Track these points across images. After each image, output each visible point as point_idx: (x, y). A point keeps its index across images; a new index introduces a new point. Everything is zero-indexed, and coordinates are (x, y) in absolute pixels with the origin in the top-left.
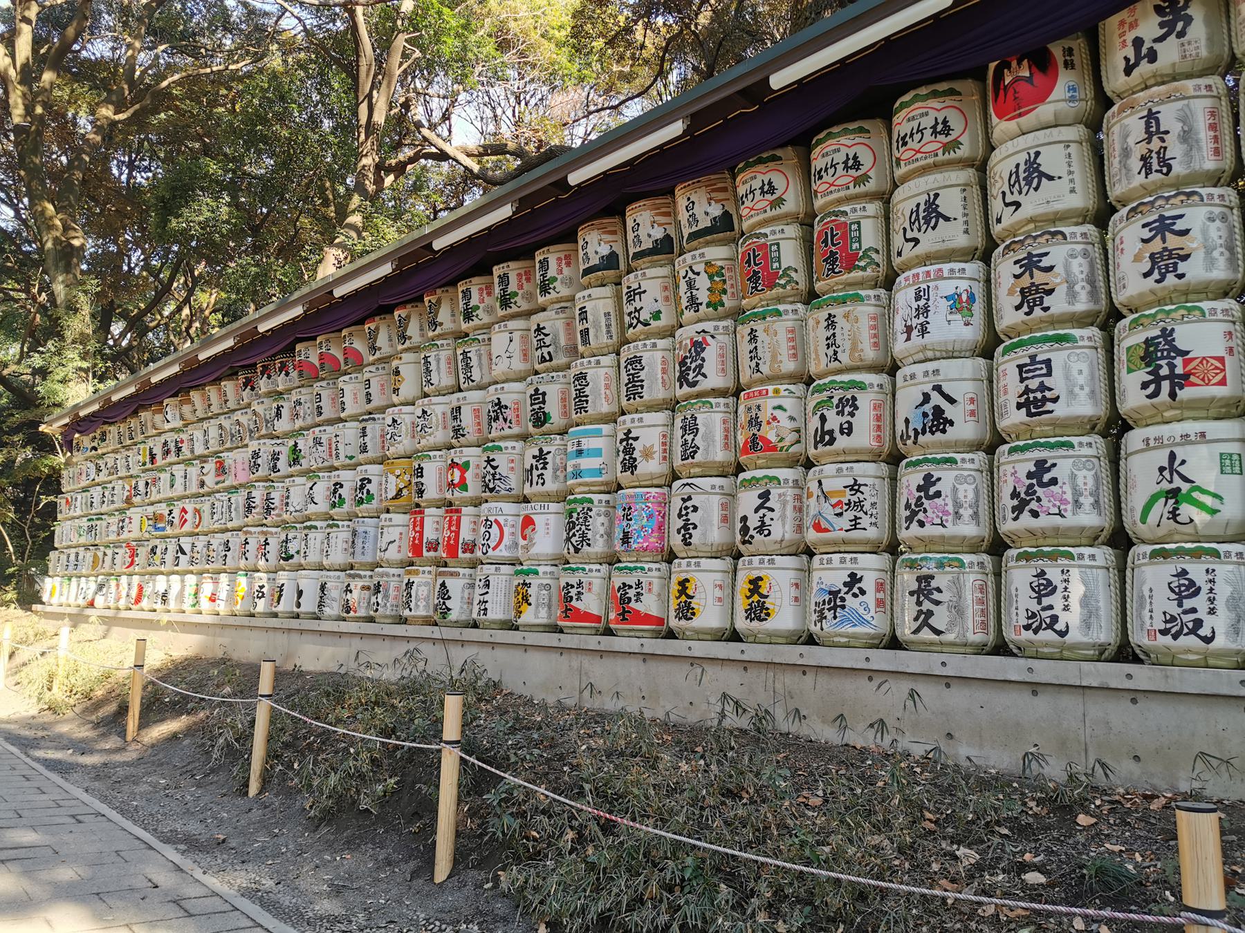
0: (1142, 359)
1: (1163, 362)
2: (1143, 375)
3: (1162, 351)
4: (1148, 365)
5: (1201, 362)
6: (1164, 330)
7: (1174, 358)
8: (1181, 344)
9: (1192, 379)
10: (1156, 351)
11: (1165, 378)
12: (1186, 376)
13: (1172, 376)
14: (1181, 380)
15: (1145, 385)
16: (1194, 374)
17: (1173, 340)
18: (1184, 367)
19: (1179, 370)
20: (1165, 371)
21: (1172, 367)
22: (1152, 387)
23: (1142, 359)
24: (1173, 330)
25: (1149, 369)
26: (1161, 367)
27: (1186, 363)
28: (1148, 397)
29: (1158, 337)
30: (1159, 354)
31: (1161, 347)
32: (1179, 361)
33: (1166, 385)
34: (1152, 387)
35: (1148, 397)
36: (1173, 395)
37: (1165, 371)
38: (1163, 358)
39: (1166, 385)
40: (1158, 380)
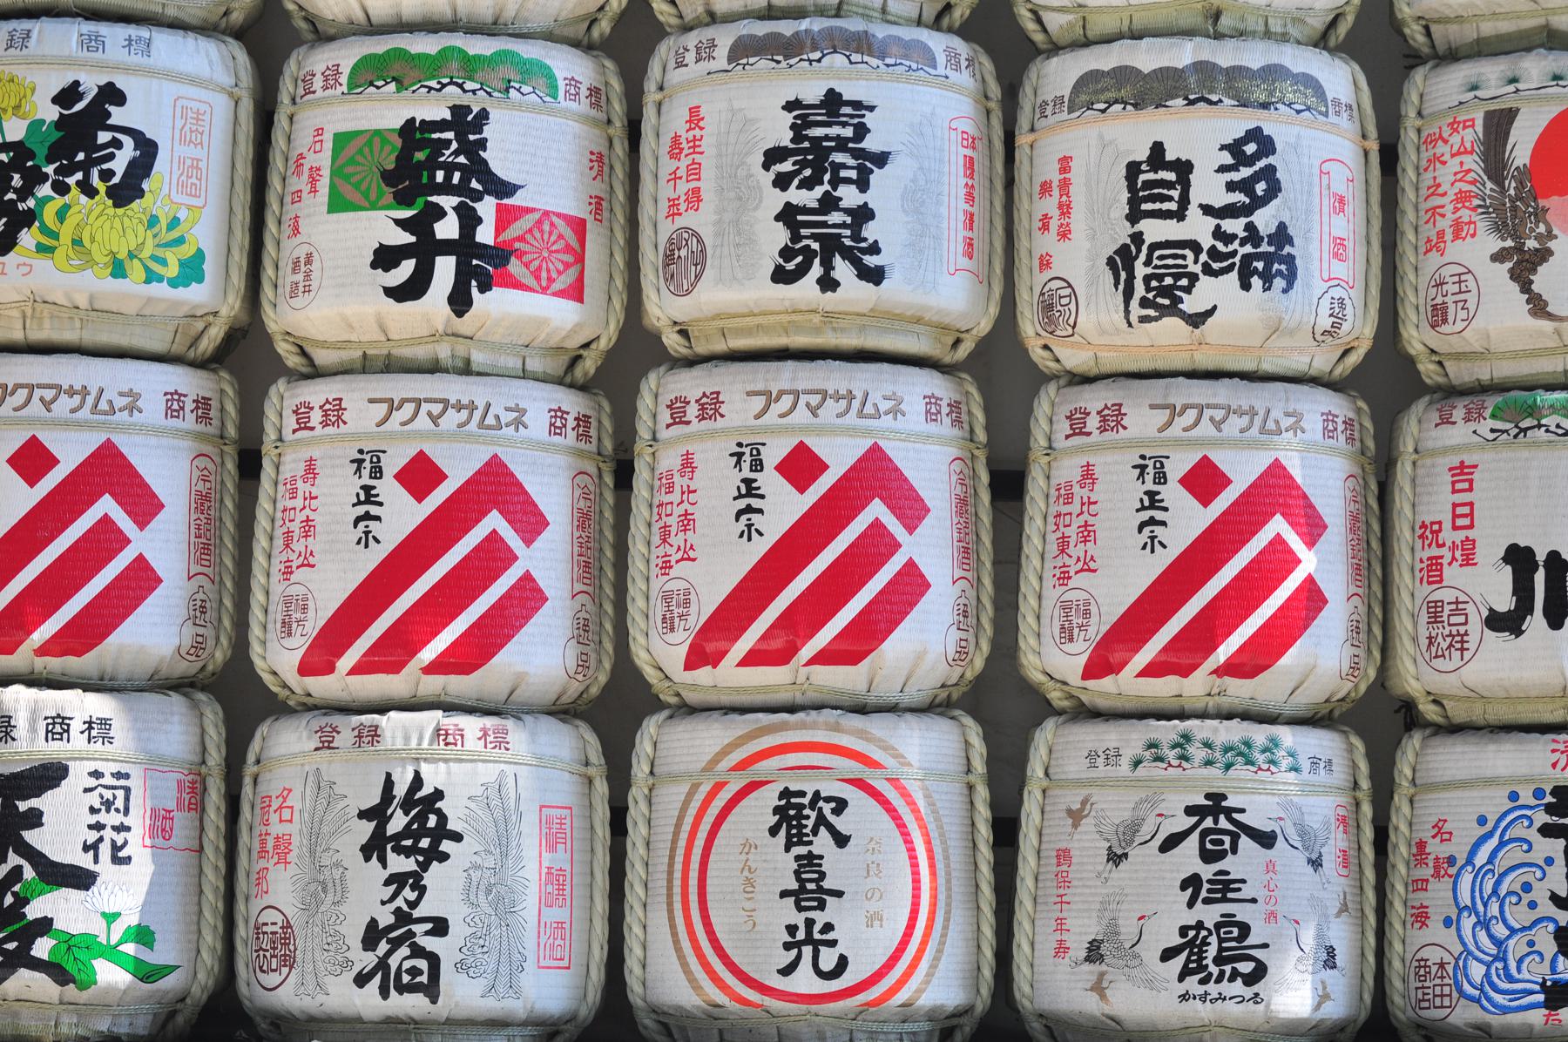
0: (388, 177)
1: (448, 202)
2: (383, 226)
3: (450, 168)
4: (403, 200)
5: (539, 223)
6: (459, 111)
7: (478, 197)
8: (498, 160)
9: (514, 267)
10: (432, 164)
11: (446, 247)
12: (500, 254)
13: (465, 247)
14: (480, 268)
15: (385, 258)
16: (520, 255)
17: (482, 144)
18: (499, 229)
19: (485, 234)
20: (447, 229)
21: (469, 220)
22: (407, 267)
23: (388, 177)
24: (483, 115)
25: (407, 213)
26: (440, 213)
27: (506, 217)
28: (390, 292)
29: (441, 125)
30: (440, 176)
31: (447, 156)
32: (487, 208)
33: (445, 267)
34: (407, 267)
35: (390, 292)
36: (460, 301)
37: (447, 229)
38: (446, 188)
39: (445, 267)
40: (426, 249)
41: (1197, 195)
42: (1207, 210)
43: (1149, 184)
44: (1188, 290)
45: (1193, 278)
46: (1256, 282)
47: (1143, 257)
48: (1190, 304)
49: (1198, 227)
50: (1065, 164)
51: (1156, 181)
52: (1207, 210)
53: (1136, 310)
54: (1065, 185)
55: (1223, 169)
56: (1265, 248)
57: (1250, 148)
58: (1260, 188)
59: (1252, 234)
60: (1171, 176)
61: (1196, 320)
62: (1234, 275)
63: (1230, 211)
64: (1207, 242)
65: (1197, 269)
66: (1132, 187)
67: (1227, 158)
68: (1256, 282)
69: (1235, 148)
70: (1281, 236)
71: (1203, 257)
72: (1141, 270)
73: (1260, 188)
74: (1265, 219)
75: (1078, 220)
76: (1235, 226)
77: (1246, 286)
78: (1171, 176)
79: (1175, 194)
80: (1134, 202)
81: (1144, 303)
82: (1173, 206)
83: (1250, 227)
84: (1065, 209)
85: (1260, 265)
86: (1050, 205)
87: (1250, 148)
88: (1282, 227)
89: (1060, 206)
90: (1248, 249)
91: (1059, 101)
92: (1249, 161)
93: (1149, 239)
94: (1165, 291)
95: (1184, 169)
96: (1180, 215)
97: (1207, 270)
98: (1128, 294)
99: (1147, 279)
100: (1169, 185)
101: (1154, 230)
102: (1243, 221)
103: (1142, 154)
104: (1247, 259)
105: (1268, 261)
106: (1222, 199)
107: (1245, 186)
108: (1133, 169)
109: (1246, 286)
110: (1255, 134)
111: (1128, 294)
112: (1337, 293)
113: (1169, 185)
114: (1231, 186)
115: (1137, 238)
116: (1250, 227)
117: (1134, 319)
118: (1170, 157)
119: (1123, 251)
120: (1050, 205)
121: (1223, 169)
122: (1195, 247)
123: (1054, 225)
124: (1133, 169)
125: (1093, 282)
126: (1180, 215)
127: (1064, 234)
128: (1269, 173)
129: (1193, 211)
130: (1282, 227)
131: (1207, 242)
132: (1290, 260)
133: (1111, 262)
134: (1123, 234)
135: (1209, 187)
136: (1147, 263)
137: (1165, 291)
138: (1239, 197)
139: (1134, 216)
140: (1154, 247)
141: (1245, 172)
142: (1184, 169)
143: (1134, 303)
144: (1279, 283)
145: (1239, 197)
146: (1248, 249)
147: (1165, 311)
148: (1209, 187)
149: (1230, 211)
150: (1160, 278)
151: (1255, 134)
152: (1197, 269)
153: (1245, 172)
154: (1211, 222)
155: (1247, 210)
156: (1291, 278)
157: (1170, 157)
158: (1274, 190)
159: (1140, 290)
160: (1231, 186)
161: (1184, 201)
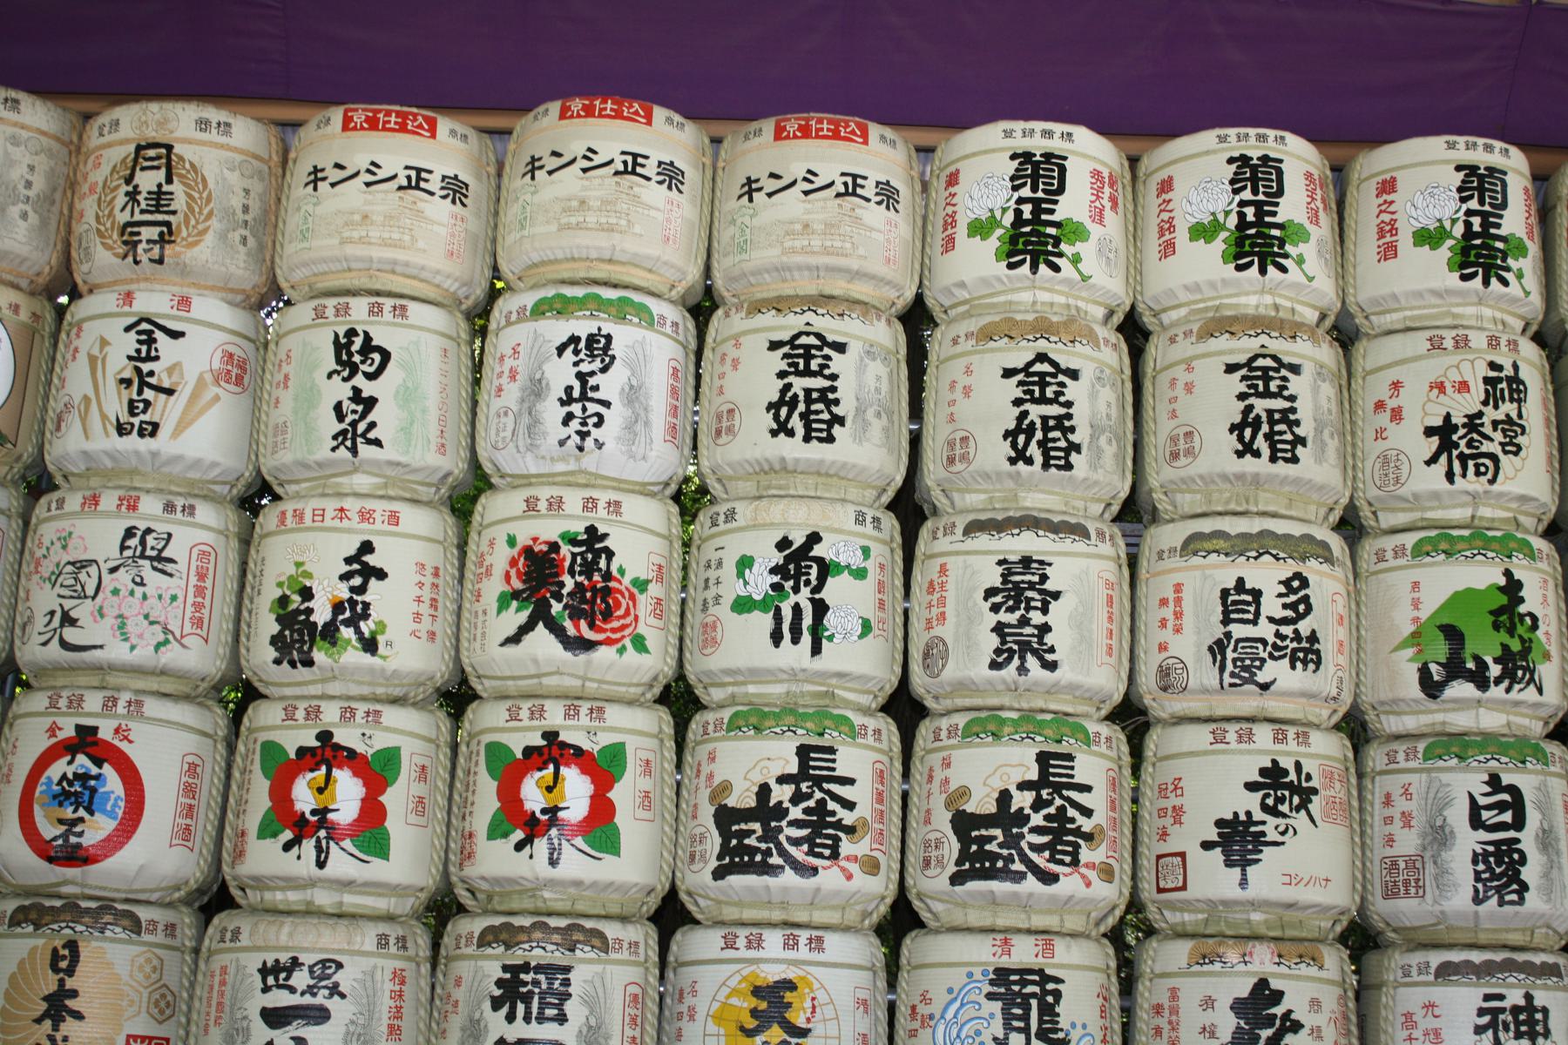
41: (1264, 611)
42: (1271, 620)
43: (1235, 603)
44: (1260, 668)
45: (1263, 661)
46: (1299, 664)
47: (1231, 646)
48: (1262, 677)
49: (1265, 630)
50: (1178, 588)
51: (1239, 601)
52: (1271, 620)
53: (1227, 679)
54: (1178, 601)
55: (1280, 595)
56: (1305, 644)
57: (1296, 584)
58: (1302, 608)
59: (1297, 636)
60: (1249, 598)
61: (1265, 687)
62: (1287, 660)
63: (1284, 621)
64: (1271, 639)
65: (1265, 655)
66: (1224, 603)
67: (1283, 589)
68: (1299, 664)
69: (1286, 583)
70: (1313, 638)
71: (1269, 648)
72: (1230, 655)
73: (1302, 608)
74: (1304, 627)
75: (1188, 621)
76: (1287, 630)
77: (1293, 667)
78: (1249, 598)
79: (1252, 609)
80: (1226, 613)
81: (1233, 675)
82: (1250, 617)
83: (1296, 631)
84: (1178, 615)
85: (1301, 655)
86: (1168, 612)
87: (1296, 584)
88: (1313, 632)
89: (1175, 613)
90: (1295, 645)
91: (1172, 550)
92: (1295, 591)
93: (1235, 636)
94: (1245, 668)
95: (1257, 594)
96: (1255, 622)
97: (1271, 656)
98: (1222, 669)
99: (1234, 661)
100: (1248, 604)
101: (1238, 631)
102: (1292, 628)
103: (1231, 584)
104: (1294, 651)
105: (1307, 653)
106: (1280, 613)
107: (1293, 606)
108: (1225, 593)
109: (1293, 667)
110: (1297, 576)
111: (1222, 669)
112: (1340, 674)
113: (1248, 604)
114: (1285, 606)
115: (1228, 635)
116: (1296, 631)
117: (1226, 684)
118: (1248, 586)
119: (1219, 643)
120: (1168, 612)
121: (1280, 595)
122: (1264, 642)
123: (1170, 625)
124: (1225, 593)
125: (1198, 660)
126: (1255, 622)
127: (1178, 630)
128: (1306, 600)
129: (1263, 620)
130: (1313, 632)
131: (1271, 639)
132: (1318, 652)
133: (1210, 649)
134: (1219, 632)
135: (1272, 606)
136: (1235, 650)
137: (1245, 668)
138: (1289, 613)
139: (1226, 621)
140: (1238, 641)
141: (1293, 598)
142: (1257, 594)
143: (1226, 675)
144: (1311, 666)
145: (1289, 613)
146: (1295, 645)
147: (1246, 681)
148: (1272, 606)
149: (1284, 621)
150: (1242, 660)
151: (1297, 576)
152: (1265, 655)
153: (1293, 598)
154: (1274, 627)
155: (1292, 621)
156: (1318, 663)
157: (1248, 586)
158: (1309, 609)
159: (1229, 667)
160: (1285, 606)
161: (1257, 614)
